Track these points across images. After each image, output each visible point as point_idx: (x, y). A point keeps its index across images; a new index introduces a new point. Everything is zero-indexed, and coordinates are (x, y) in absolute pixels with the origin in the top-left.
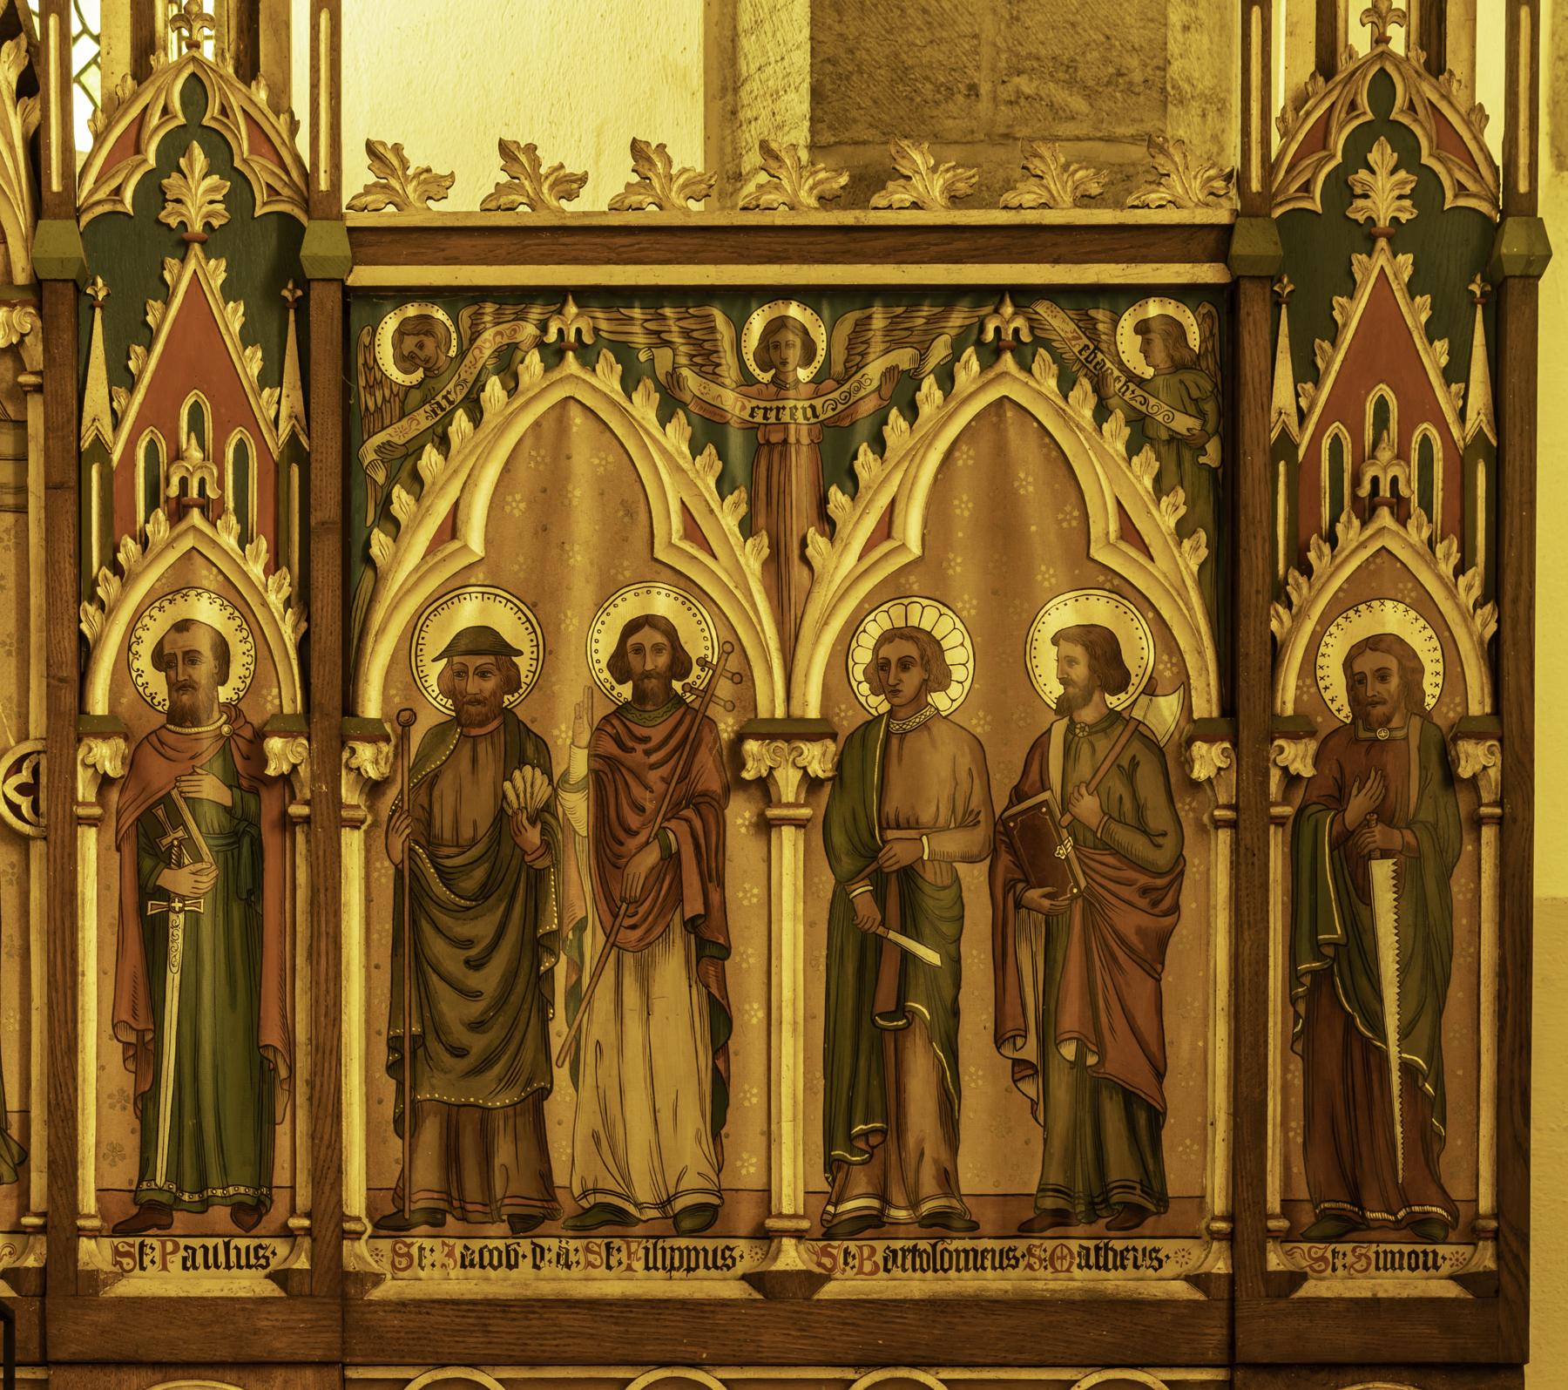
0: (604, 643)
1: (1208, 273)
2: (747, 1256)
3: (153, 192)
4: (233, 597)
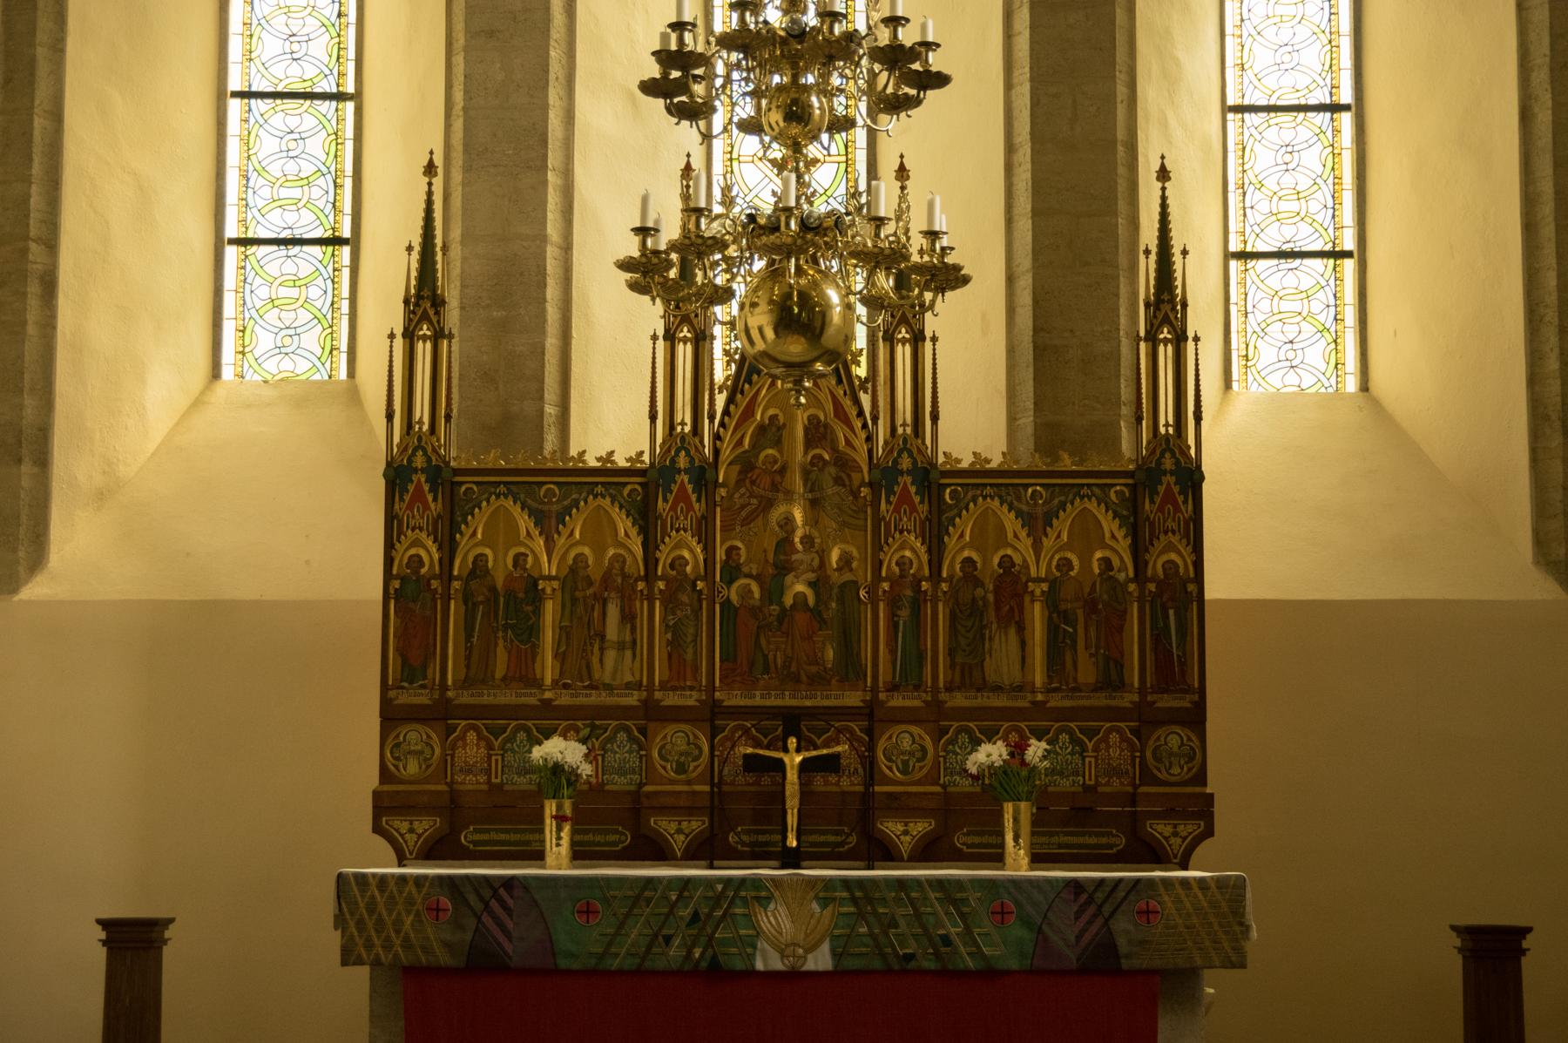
0: (996, 560)
1: (1130, 481)
2: (1029, 697)
3: (895, 462)
4: (913, 550)
